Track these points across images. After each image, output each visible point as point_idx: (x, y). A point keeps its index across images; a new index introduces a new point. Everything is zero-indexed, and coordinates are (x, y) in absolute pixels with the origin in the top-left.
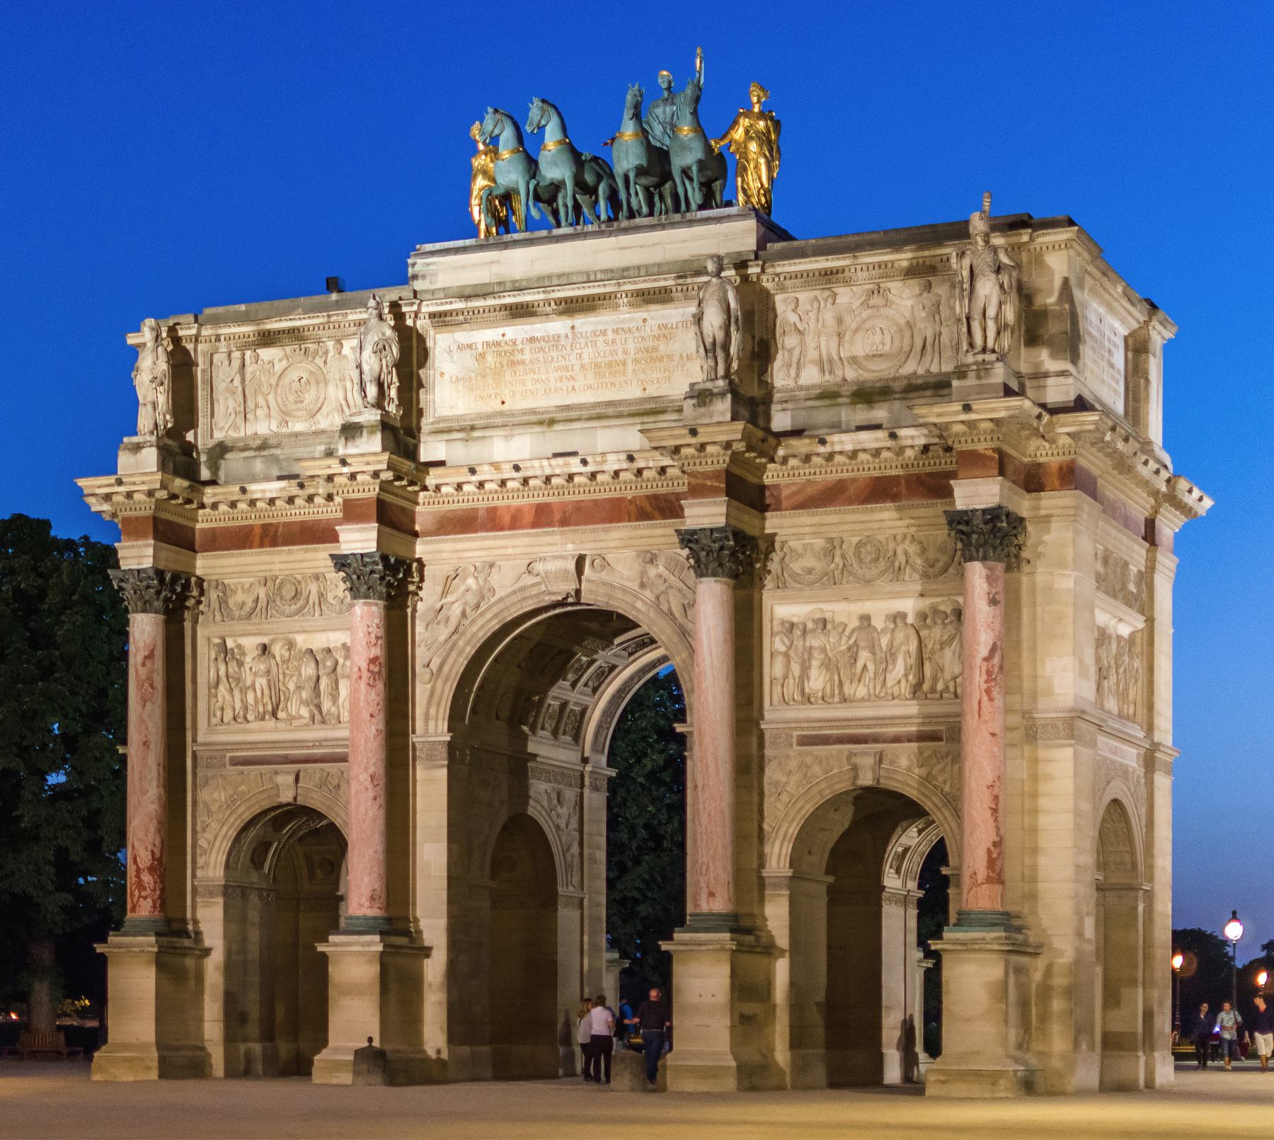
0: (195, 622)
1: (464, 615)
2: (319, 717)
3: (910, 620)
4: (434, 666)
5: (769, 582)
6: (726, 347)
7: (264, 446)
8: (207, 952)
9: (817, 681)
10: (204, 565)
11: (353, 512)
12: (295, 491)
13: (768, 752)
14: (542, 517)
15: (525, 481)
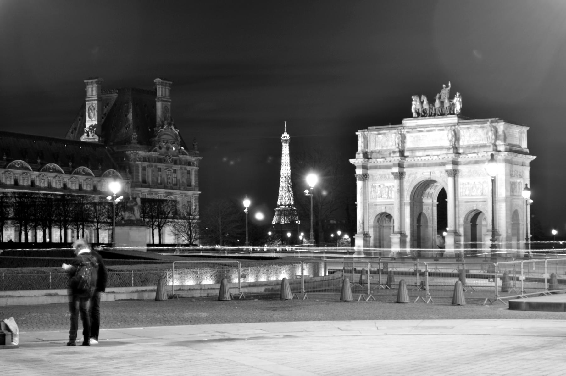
0: (368, 181)
1: (412, 181)
2: (389, 198)
3: (482, 183)
4: (408, 189)
5: (460, 177)
6: (452, 141)
7: (379, 152)
8: (370, 237)
9: (467, 193)
10: (369, 172)
11: (394, 165)
12: (385, 160)
13: (460, 204)
14: (424, 165)
15: (422, 160)
